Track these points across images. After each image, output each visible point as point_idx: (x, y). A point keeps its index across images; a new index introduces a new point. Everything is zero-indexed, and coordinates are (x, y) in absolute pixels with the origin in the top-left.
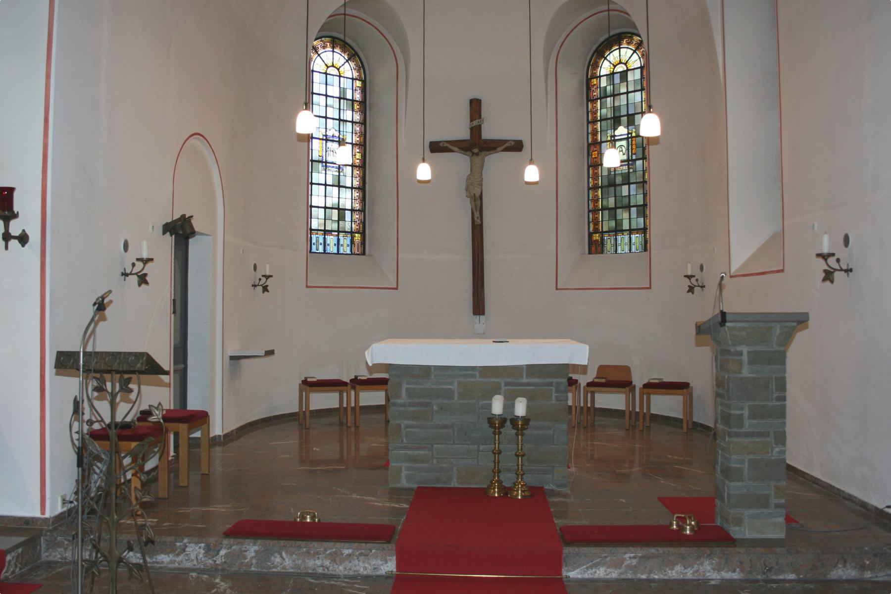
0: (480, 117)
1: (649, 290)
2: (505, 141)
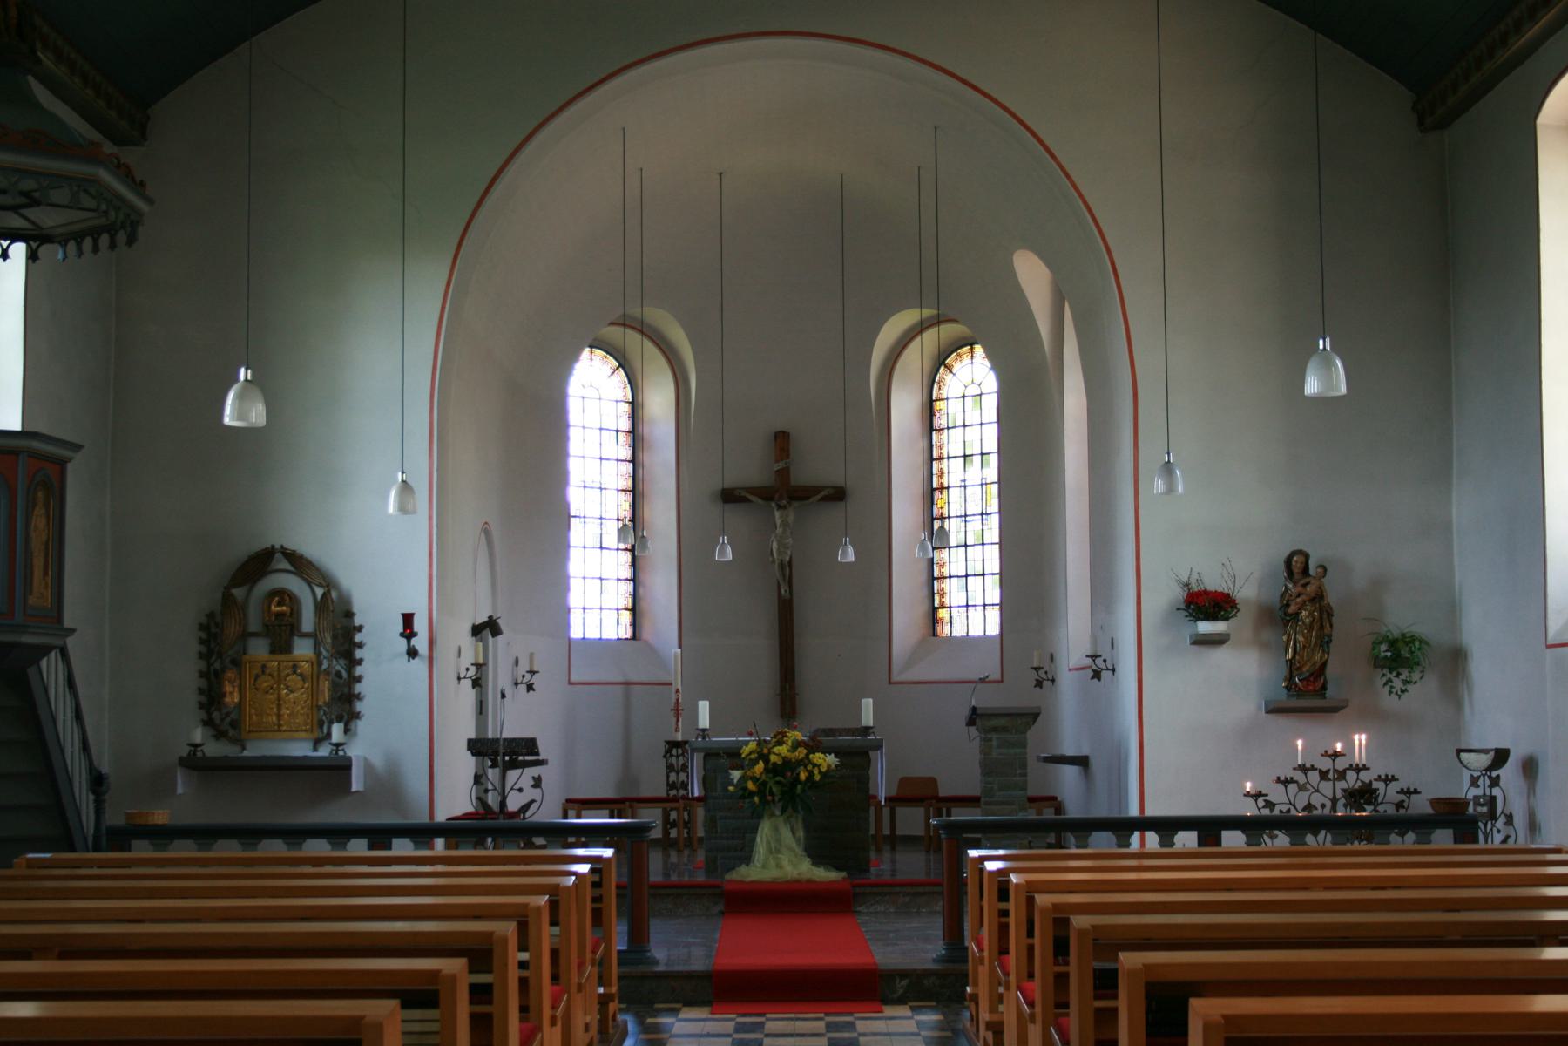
0: (788, 457)
1: (1001, 684)
2: (823, 488)
